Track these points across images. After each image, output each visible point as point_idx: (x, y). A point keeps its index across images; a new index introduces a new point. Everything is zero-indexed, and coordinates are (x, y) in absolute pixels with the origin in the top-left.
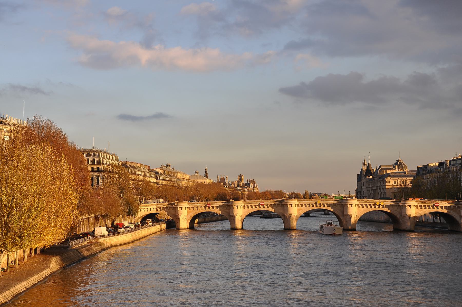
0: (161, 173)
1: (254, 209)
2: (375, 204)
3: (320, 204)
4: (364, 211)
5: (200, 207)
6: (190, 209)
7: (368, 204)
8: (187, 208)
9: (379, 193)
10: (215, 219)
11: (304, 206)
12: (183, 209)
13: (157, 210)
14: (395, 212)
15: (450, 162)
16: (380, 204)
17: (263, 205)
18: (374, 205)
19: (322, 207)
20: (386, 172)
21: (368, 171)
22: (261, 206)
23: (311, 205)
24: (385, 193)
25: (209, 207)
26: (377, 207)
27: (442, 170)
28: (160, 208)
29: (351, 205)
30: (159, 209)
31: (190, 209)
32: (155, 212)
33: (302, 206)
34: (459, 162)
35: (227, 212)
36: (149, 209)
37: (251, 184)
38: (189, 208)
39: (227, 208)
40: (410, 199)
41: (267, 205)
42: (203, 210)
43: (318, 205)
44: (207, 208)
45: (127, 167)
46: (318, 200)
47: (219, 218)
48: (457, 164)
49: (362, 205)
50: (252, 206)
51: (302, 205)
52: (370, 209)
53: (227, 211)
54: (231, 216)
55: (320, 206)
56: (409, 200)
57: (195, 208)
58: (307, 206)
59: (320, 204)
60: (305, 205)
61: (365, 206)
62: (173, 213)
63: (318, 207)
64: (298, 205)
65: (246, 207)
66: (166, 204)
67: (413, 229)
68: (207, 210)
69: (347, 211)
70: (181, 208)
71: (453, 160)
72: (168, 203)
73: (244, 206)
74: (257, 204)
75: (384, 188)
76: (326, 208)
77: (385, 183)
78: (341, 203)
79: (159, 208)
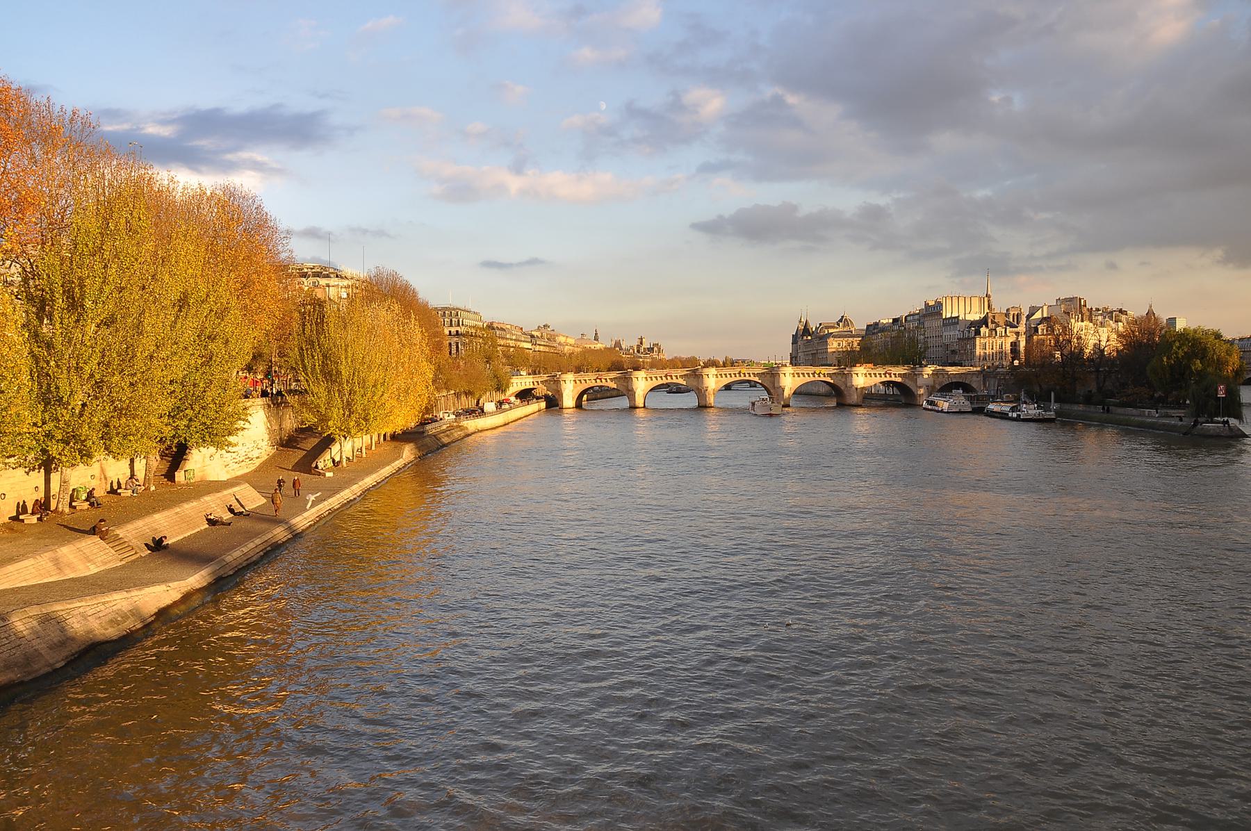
1: (660, 382)
2: (815, 372)
3: (744, 374)
4: (800, 381)
5: (590, 380)
8: (572, 382)
11: (724, 376)
13: (534, 384)
14: (838, 382)
15: (906, 317)
17: (671, 376)
18: (813, 374)
19: (747, 378)
21: (806, 331)
23: (733, 376)
26: (816, 376)
27: (896, 327)
28: (538, 382)
30: (536, 383)
31: (576, 383)
32: (532, 386)
33: (722, 377)
34: (916, 317)
35: (623, 385)
36: (523, 384)
37: (655, 349)
38: (575, 381)
40: (857, 365)
41: (676, 376)
42: (593, 384)
43: (742, 375)
44: (598, 381)
45: (493, 329)
47: (615, 393)
48: (914, 320)
49: (798, 374)
50: (656, 377)
51: (721, 375)
52: (807, 379)
55: (745, 376)
56: (856, 366)
57: (583, 381)
58: (728, 376)
59: (744, 374)
61: (801, 375)
62: (555, 387)
63: (742, 378)
65: (649, 379)
66: (545, 377)
67: (860, 404)
69: (779, 382)
71: (909, 315)
73: (646, 378)
76: (752, 378)
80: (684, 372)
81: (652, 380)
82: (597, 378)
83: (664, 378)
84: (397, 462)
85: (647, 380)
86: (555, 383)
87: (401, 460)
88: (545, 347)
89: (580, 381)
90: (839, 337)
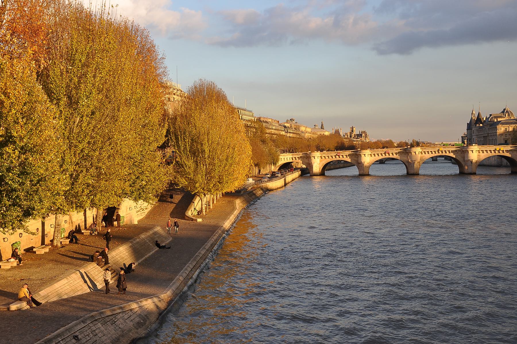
0: (288, 126)
1: (381, 157)
2: (496, 150)
3: (442, 151)
4: (484, 156)
5: (332, 156)
6: (322, 158)
7: (488, 149)
9: (489, 140)
10: (350, 165)
11: (427, 153)
12: (316, 158)
13: (293, 159)
16: (500, 150)
17: (389, 153)
18: (495, 151)
19: (444, 154)
20: (497, 120)
21: (479, 120)
22: (387, 154)
23: (433, 152)
24: (496, 139)
25: (339, 156)
26: (497, 152)
28: (295, 158)
29: (472, 151)
30: (294, 159)
31: (322, 158)
32: (291, 161)
33: (425, 154)
35: (355, 160)
36: (286, 159)
37: (363, 135)
38: (321, 157)
39: (355, 157)
41: (392, 153)
42: (334, 159)
43: (440, 152)
44: (337, 157)
46: (440, 147)
47: (349, 165)
49: (483, 151)
50: (378, 154)
51: (425, 152)
52: (490, 154)
53: (356, 159)
54: (359, 164)
57: (327, 157)
58: (430, 153)
59: (442, 151)
60: (428, 152)
61: (485, 152)
63: (440, 154)
64: (422, 152)
65: (373, 155)
66: (301, 154)
68: (338, 158)
69: (468, 157)
70: (314, 157)
72: (302, 153)
73: (371, 155)
74: (383, 153)
75: (495, 135)
76: (448, 154)
77: (497, 131)
78: (462, 149)
79: (489, 150)
80: (398, 150)
81: (375, 156)
82: (337, 155)
83: (383, 155)
84: (235, 212)
85: (371, 156)
86: (307, 159)
87: (237, 210)
88: (293, 134)
89: (325, 157)
90: (506, 124)
